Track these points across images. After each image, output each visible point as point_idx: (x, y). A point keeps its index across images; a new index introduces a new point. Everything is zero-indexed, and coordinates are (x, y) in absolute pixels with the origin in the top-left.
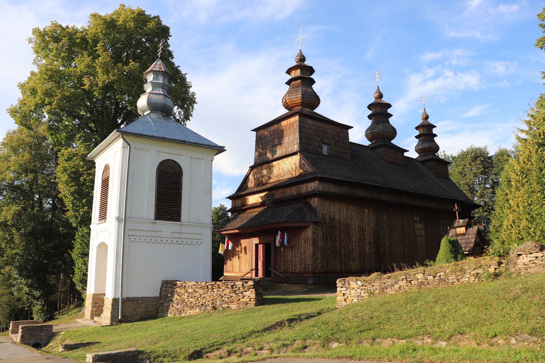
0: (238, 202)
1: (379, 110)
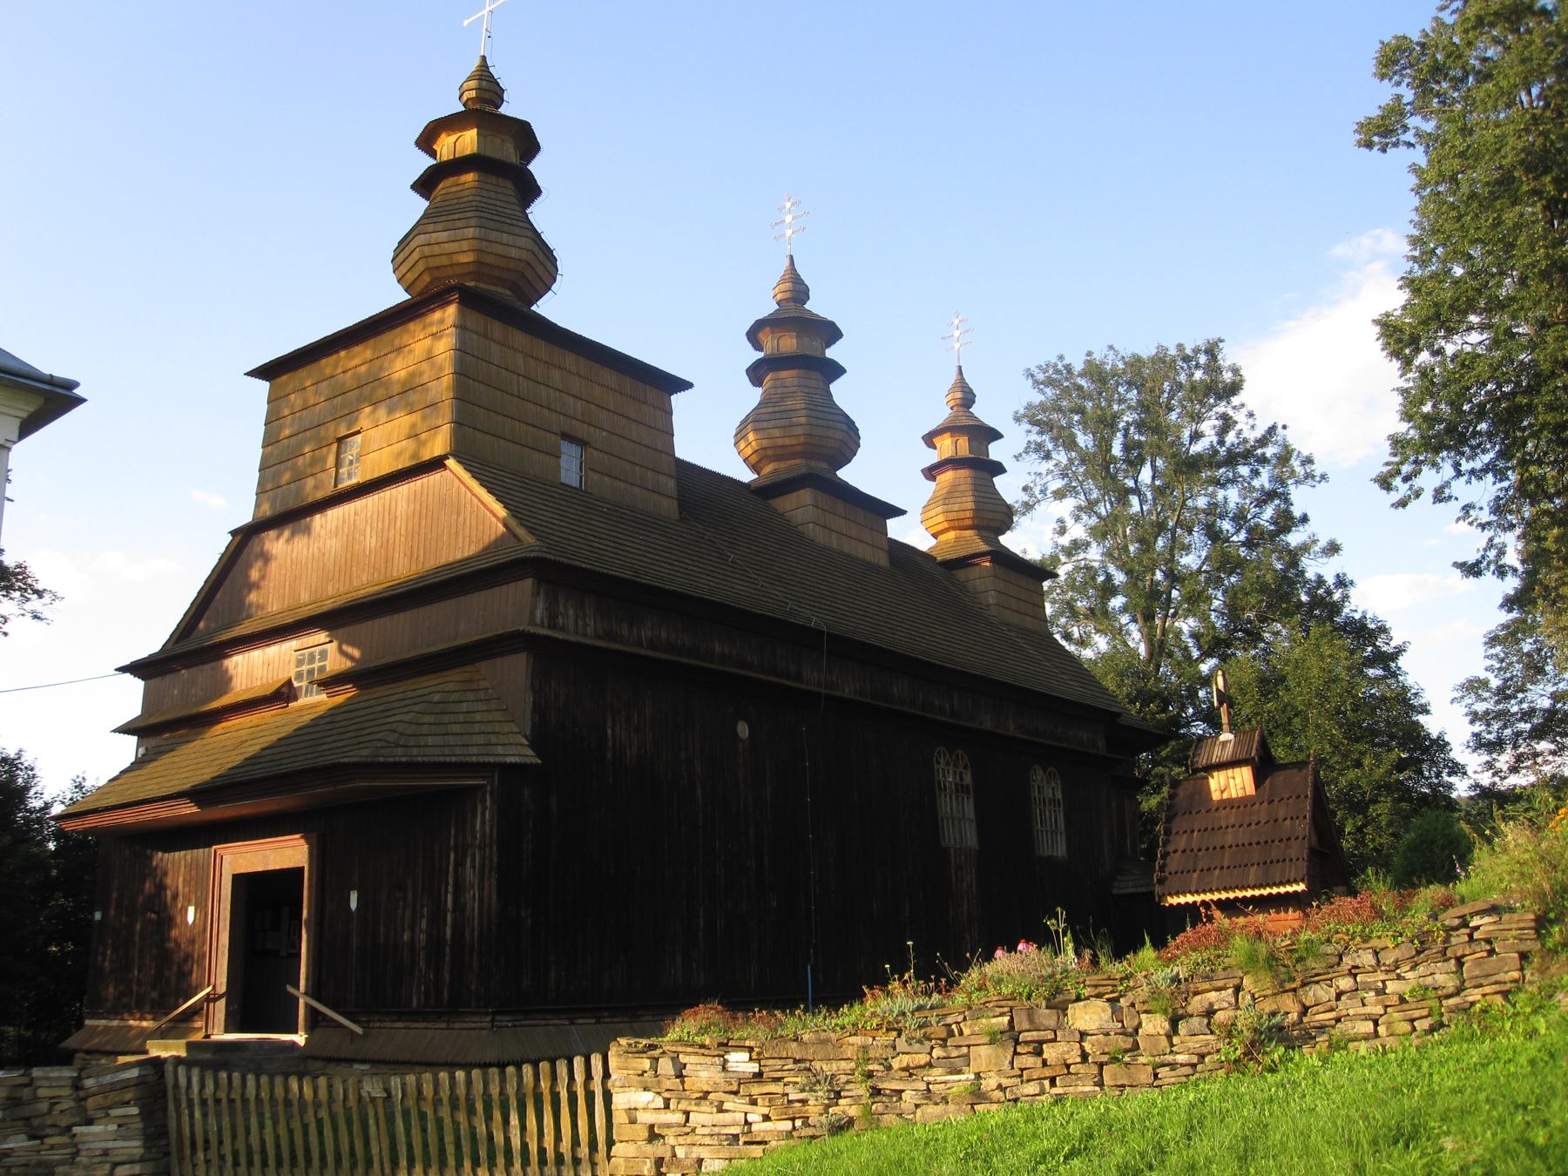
0: (176, 683)
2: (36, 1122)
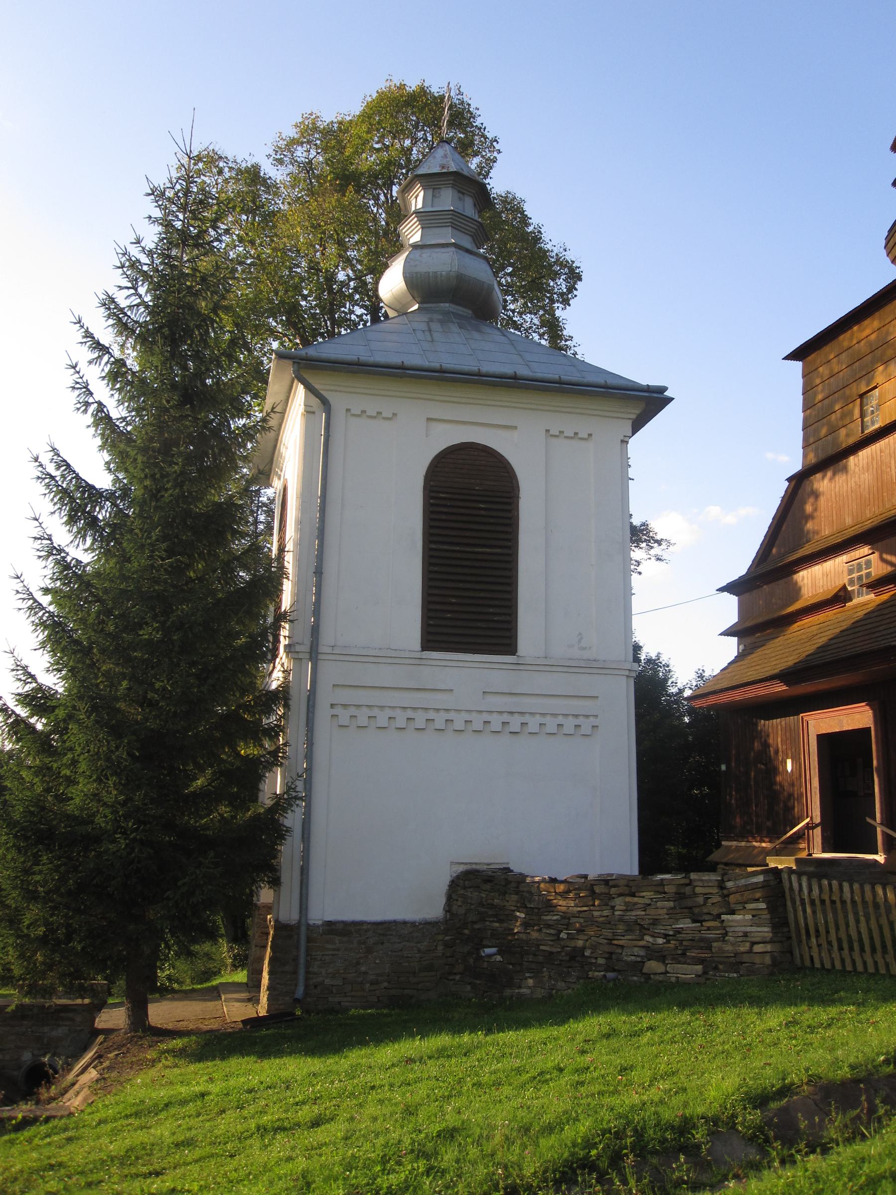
2: (696, 910)
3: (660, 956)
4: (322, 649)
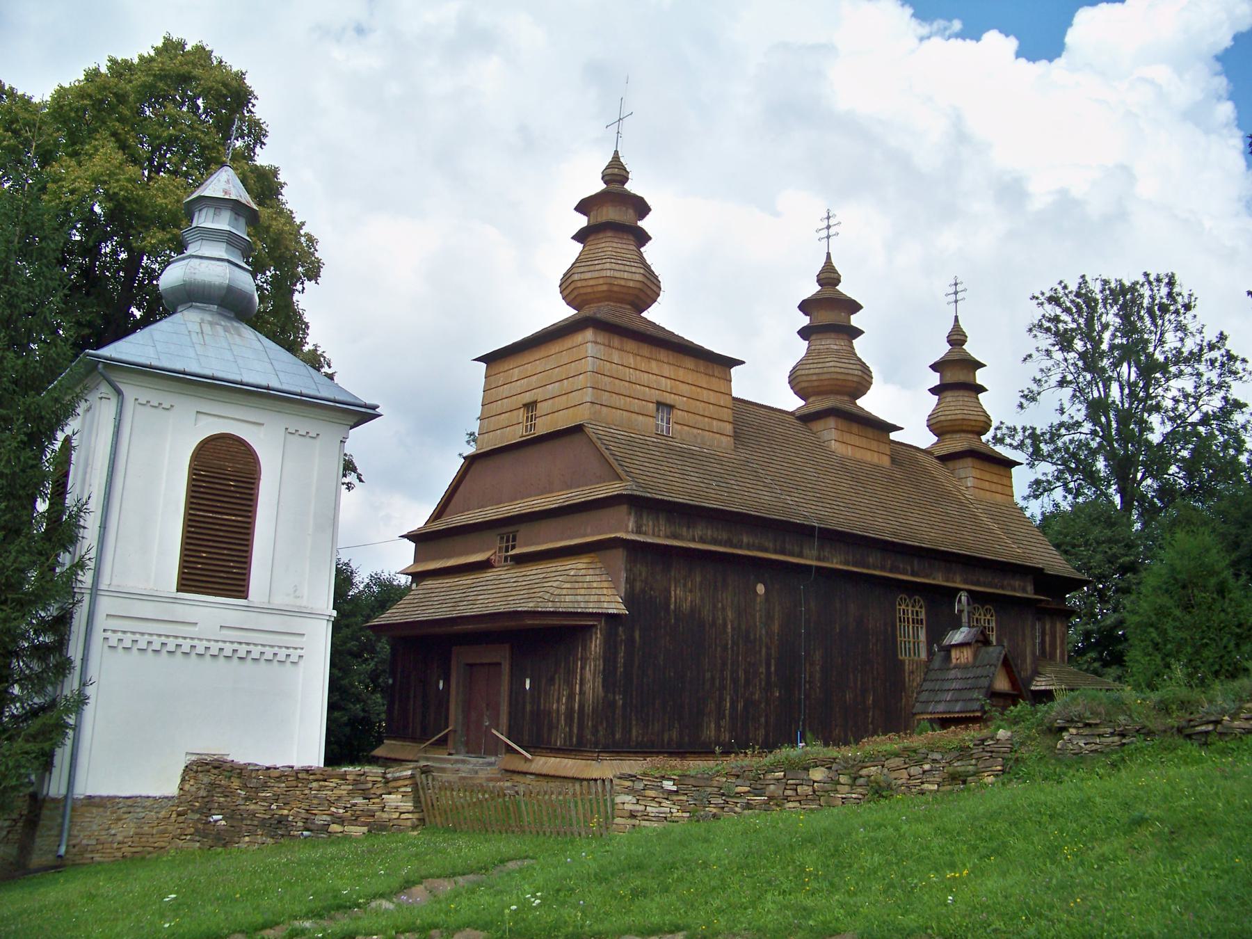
1: (826, 317)
3: (341, 821)
4: (102, 587)
